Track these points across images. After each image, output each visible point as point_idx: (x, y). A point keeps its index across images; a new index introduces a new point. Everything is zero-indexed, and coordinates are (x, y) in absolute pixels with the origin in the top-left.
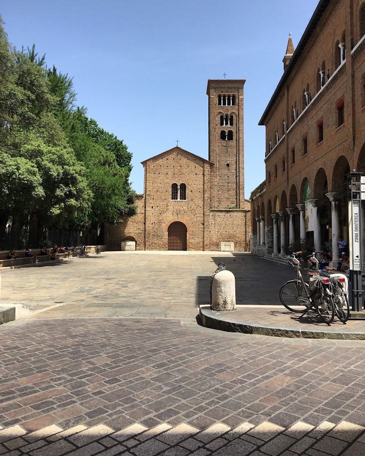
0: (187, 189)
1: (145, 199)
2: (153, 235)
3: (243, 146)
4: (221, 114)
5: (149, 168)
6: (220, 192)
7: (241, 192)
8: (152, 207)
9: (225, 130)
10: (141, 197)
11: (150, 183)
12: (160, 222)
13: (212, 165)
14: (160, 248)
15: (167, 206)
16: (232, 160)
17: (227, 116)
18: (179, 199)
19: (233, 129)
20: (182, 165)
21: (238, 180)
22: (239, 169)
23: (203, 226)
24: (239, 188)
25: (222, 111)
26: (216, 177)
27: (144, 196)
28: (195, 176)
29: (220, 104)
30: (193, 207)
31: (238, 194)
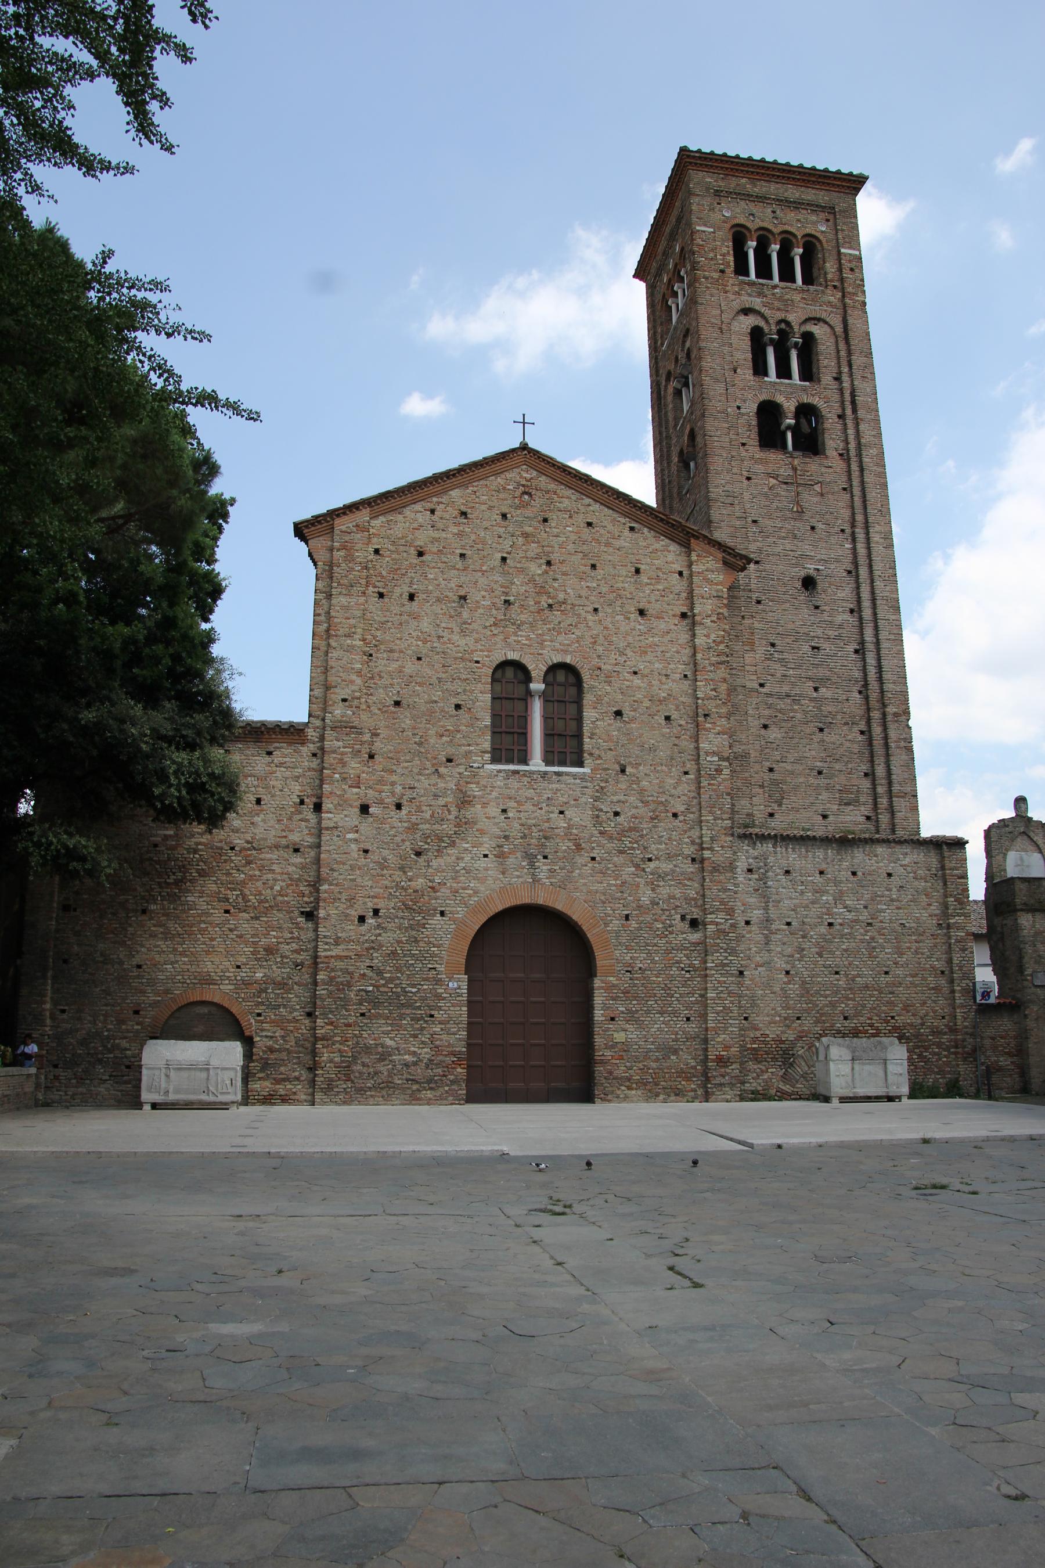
0: (588, 699)
1: (319, 754)
2: (366, 997)
3: (885, 486)
4: (751, 321)
5: (350, 558)
8: (364, 809)
9: (780, 399)
10: (291, 733)
11: (350, 649)
12: (416, 908)
13: (735, 561)
14: (414, 1087)
15: (464, 801)
16: (829, 557)
17: (784, 334)
18: (537, 763)
19: (823, 397)
20: (554, 557)
21: (872, 671)
22: (874, 606)
23: (695, 937)
24: (884, 715)
25: (757, 303)
26: (752, 644)
27: (310, 732)
28: (641, 624)
29: (741, 269)
31: (879, 750)
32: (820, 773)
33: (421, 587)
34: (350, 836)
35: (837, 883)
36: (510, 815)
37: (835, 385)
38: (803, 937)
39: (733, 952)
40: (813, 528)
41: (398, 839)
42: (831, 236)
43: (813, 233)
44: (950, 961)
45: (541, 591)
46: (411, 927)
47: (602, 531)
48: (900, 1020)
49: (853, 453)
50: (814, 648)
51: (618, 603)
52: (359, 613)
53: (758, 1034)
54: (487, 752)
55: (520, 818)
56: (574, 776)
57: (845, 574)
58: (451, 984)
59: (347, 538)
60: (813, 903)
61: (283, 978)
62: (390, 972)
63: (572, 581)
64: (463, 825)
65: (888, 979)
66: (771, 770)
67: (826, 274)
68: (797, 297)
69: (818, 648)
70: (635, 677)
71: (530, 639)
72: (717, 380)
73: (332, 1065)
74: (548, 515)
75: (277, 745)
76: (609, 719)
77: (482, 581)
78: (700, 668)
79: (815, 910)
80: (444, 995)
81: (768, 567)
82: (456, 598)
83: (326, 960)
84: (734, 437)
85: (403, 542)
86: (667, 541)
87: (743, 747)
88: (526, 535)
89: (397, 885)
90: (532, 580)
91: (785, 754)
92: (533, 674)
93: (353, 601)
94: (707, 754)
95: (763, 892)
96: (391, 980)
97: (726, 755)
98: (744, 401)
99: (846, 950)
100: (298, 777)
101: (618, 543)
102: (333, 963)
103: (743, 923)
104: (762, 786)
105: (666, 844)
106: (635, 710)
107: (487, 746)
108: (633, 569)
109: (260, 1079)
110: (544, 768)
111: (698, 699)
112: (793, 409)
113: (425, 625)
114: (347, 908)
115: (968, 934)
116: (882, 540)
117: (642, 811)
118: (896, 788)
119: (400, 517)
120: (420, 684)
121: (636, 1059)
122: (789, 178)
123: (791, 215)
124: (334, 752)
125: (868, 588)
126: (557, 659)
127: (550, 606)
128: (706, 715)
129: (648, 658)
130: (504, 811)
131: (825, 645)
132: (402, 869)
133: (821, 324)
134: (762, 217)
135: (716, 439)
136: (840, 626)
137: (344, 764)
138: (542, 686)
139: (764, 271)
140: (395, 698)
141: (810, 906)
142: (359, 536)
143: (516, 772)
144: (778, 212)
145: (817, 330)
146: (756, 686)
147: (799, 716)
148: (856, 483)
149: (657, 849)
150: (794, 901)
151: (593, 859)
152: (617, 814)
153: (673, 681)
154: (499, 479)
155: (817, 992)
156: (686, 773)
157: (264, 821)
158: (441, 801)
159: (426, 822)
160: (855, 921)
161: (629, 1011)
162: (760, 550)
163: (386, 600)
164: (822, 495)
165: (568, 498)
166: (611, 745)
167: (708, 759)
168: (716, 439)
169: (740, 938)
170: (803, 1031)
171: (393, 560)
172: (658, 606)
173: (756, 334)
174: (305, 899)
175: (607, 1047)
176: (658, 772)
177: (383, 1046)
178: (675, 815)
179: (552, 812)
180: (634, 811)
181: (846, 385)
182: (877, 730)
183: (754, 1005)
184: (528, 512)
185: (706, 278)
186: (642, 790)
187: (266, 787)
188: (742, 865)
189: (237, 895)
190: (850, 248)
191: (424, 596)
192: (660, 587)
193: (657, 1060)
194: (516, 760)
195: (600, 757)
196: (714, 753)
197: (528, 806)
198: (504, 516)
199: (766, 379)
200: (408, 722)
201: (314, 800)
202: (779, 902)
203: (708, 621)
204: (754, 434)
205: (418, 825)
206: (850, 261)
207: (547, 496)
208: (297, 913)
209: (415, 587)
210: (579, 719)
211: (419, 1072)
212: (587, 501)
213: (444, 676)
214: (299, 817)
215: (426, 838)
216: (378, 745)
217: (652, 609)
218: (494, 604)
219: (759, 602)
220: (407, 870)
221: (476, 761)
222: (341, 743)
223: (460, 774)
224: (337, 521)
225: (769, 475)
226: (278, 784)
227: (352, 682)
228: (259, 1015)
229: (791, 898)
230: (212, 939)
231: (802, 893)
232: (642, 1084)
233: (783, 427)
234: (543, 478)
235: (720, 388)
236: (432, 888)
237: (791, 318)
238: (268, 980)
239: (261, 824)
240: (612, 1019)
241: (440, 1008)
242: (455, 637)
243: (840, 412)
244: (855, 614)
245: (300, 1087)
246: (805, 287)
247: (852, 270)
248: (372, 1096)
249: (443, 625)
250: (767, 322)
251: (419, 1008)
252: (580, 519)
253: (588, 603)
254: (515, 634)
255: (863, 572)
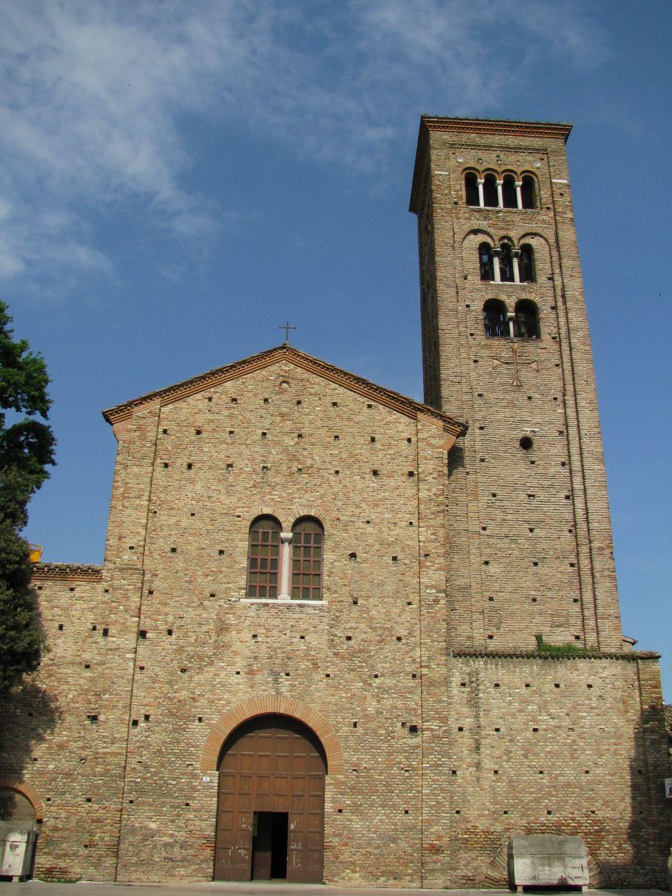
0: (328, 544)
4: (481, 238)
5: (143, 438)
6: (494, 569)
7: (597, 566)
8: (143, 634)
9: (502, 297)
15: (223, 628)
17: (506, 248)
18: (284, 597)
19: (539, 294)
20: (303, 431)
23: (416, 741)
25: (483, 224)
28: (373, 483)
29: (472, 199)
30: (357, 637)
31: (587, 579)
32: (534, 600)
33: (197, 458)
34: (129, 656)
35: (539, 693)
36: (259, 639)
37: (550, 283)
38: (511, 741)
39: (446, 755)
40: (530, 398)
41: (168, 659)
42: (546, 171)
43: (530, 169)
44: (645, 761)
45: (294, 458)
46: (174, 730)
47: (345, 409)
48: (600, 815)
49: (563, 335)
50: (530, 496)
51: (356, 466)
52: (147, 480)
53: (469, 826)
54: (243, 589)
55: (268, 642)
56: (314, 607)
57: (557, 434)
58: (204, 778)
59: (141, 422)
60: (520, 711)
61: (70, 770)
62: (155, 767)
63: (317, 450)
64: (221, 647)
65: (589, 777)
66: (491, 599)
67: (540, 199)
68: (517, 218)
69: (533, 496)
70: (368, 525)
71: (282, 497)
72: (449, 286)
73: (103, 843)
74: (301, 398)
75: (78, 583)
76: (345, 561)
77: (246, 452)
78: (422, 516)
79: (521, 718)
80: (199, 787)
81: (491, 431)
82: (224, 466)
83: (103, 756)
84: (464, 329)
85: (185, 423)
86: (399, 414)
87: (466, 580)
88: (282, 415)
89: (165, 697)
90: (286, 451)
91: (504, 585)
92: (284, 525)
93: (143, 470)
94: (427, 587)
95: (473, 702)
96: (156, 774)
97: (443, 587)
98: (473, 301)
99: (549, 752)
100: (93, 608)
101: (357, 419)
102: (109, 759)
103: (456, 730)
104: (482, 613)
105: (390, 663)
106: (367, 553)
107: (243, 583)
108: (369, 438)
109: (45, 853)
110: (289, 601)
111: (420, 541)
112: (514, 305)
113: (199, 487)
114: (122, 714)
115: (662, 737)
116: (588, 405)
117: (371, 635)
118: (600, 611)
119: (184, 405)
120: (193, 535)
121: (360, 846)
122: (509, 131)
123: (512, 158)
124: (120, 589)
125: (577, 445)
126: (304, 512)
127: (300, 470)
128: (426, 555)
129: (379, 510)
130: (255, 636)
131: (541, 495)
132: (170, 683)
133: (537, 238)
134: (489, 160)
135: (447, 331)
136: (553, 477)
137: (127, 598)
138: (290, 535)
139: (491, 200)
140: (172, 546)
141: (518, 714)
142: (151, 420)
143: (267, 605)
144: (501, 156)
145: (534, 242)
146: (478, 529)
147: (516, 552)
148: (566, 359)
149: (383, 667)
150: (503, 710)
151: (328, 676)
152: (349, 638)
153: (400, 528)
154: (264, 373)
155: (523, 790)
156: (409, 604)
157: (64, 642)
158: (204, 628)
159: (191, 644)
160: (557, 727)
161: (355, 804)
162: (484, 418)
163: (170, 468)
164: (538, 371)
165: (319, 384)
166: (345, 581)
167: (428, 591)
168: (447, 331)
169: (451, 744)
170: (509, 824)
171: (177, 437)
172: (389, 467)
173: (484, 248)
174: (92, 706)
175: (335, 835)
176: (385, 603)
177: (146, 828)
178: (399, 639)
179: (294, 637)
180: (364, 636)
181: (558, 283)
182: (585, 562)
183: (465, 800)
184: (285, 397)
185: (441, 209)
186: (372, 618)
187: (68, 616)
188: (456, 680)
189: (39, 702)
190: (560, 179)
191: (199, 465)
192: (391, 452)
193: (378, 847)
194: (258, 595)
195: (336, 592)
196: (432, 587)
197: (275, 633)
198: (266, 400)
199: (491, 282)
200: (181, 565)
201: (104, 626)
202: (489, 711)
203: (430, 478)
204: (481, 326)
205: (184, 647)
206: (560, 188)
207: (301, 384)
208: (84, 717)
209: (192, 458)
210: (319, 563)
211: (177, 852)
212: (334, 386)
213: (211, 528)
214: (90, 640)
215: (190, 658)
216: (157, 584)
217: (384, 471)
218: (254, 470)
219: (482, 460)
220: (173, 683)
221: (234, 595)
222: (126, 582)
223: (220, 606)
224: (136, 409)
225: (494, 358)
226: (77, 614)
227: (139, 533)
228: (49, 799)
229: (500, 708)
230: (17, 737)
231: (510, 703)
232: (362, 867)
233: (506, 319)
234: (299, 370)
235: (452, 292)
236: (193, 699)
237: (515, 234)
238: (57, 771)
239: (62, 645)
240: (340, 811)
241: (194, 798)
242: (222, 497)
243: (553, 304)
244: (567, 467)
245: (76, 861)
246: (524, 211)
247: (562, 194)
248: (134, 871)
249: (214, 487)
250: (491, 237)
251: (177, 798)
252: (328, 401)
253: (330, 467)
254: (270, 493)
255: (573, 431)
